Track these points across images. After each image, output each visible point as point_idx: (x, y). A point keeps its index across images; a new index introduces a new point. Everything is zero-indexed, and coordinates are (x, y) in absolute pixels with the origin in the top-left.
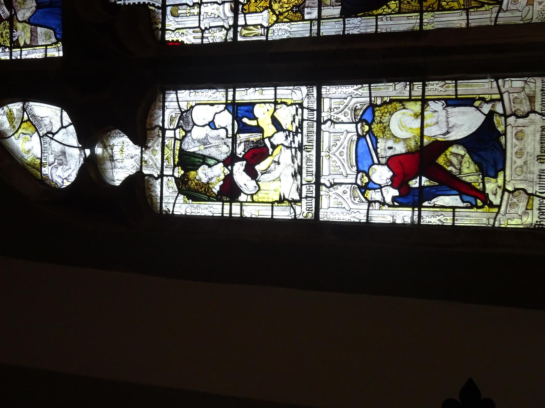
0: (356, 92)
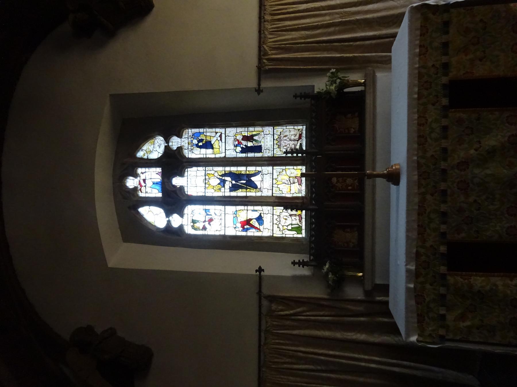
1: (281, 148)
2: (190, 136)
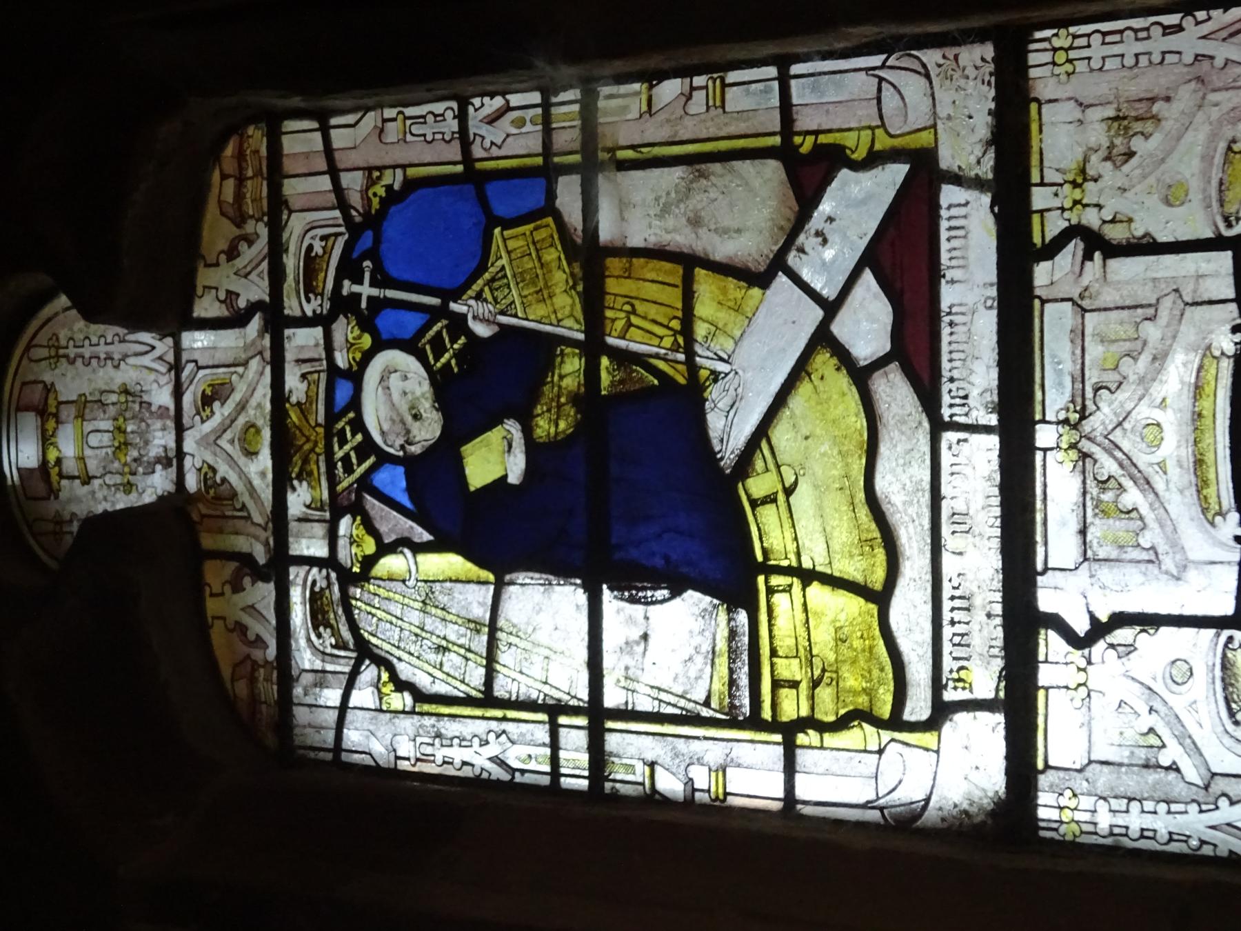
2: (311, 265)
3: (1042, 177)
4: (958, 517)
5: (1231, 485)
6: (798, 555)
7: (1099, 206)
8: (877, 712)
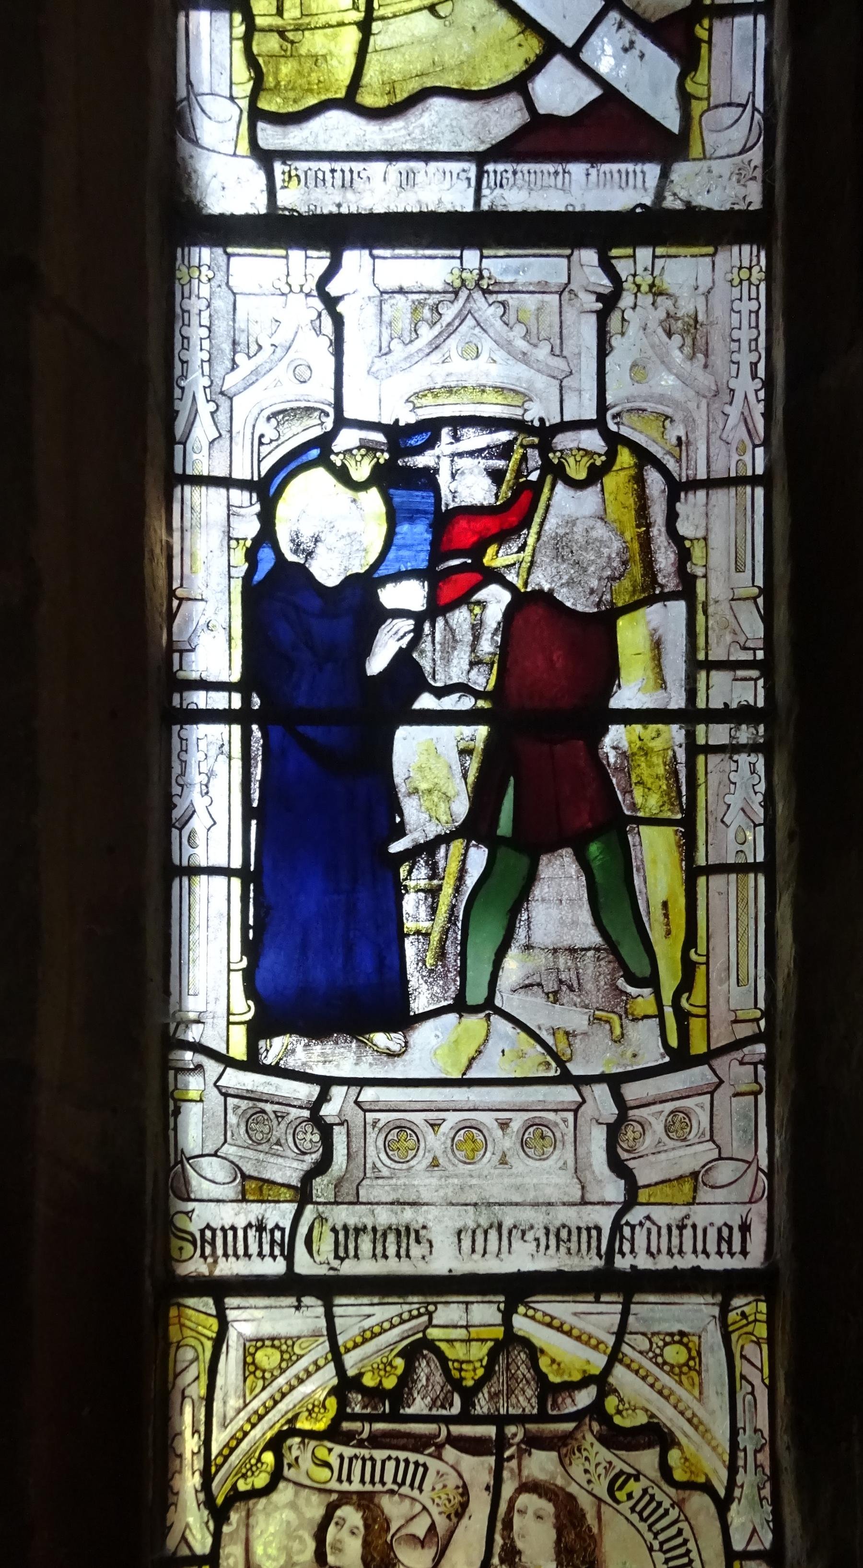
0: (734, 412)
1: (334, 1453)
3: (659, 257)
4: (410, 176)
5: (434, 416)
6: (383, 18)
7: (634, 307)
8: (263, 95)
